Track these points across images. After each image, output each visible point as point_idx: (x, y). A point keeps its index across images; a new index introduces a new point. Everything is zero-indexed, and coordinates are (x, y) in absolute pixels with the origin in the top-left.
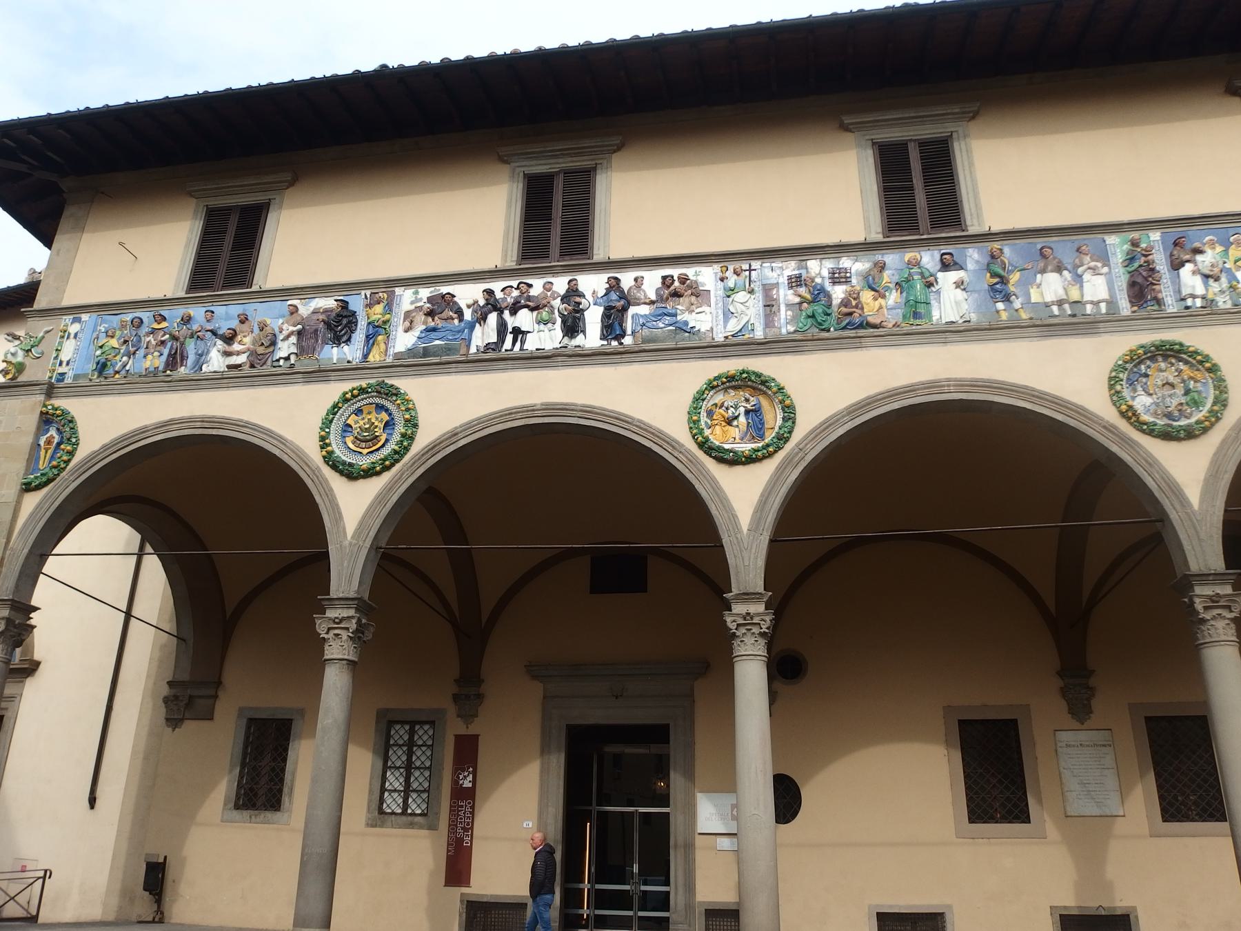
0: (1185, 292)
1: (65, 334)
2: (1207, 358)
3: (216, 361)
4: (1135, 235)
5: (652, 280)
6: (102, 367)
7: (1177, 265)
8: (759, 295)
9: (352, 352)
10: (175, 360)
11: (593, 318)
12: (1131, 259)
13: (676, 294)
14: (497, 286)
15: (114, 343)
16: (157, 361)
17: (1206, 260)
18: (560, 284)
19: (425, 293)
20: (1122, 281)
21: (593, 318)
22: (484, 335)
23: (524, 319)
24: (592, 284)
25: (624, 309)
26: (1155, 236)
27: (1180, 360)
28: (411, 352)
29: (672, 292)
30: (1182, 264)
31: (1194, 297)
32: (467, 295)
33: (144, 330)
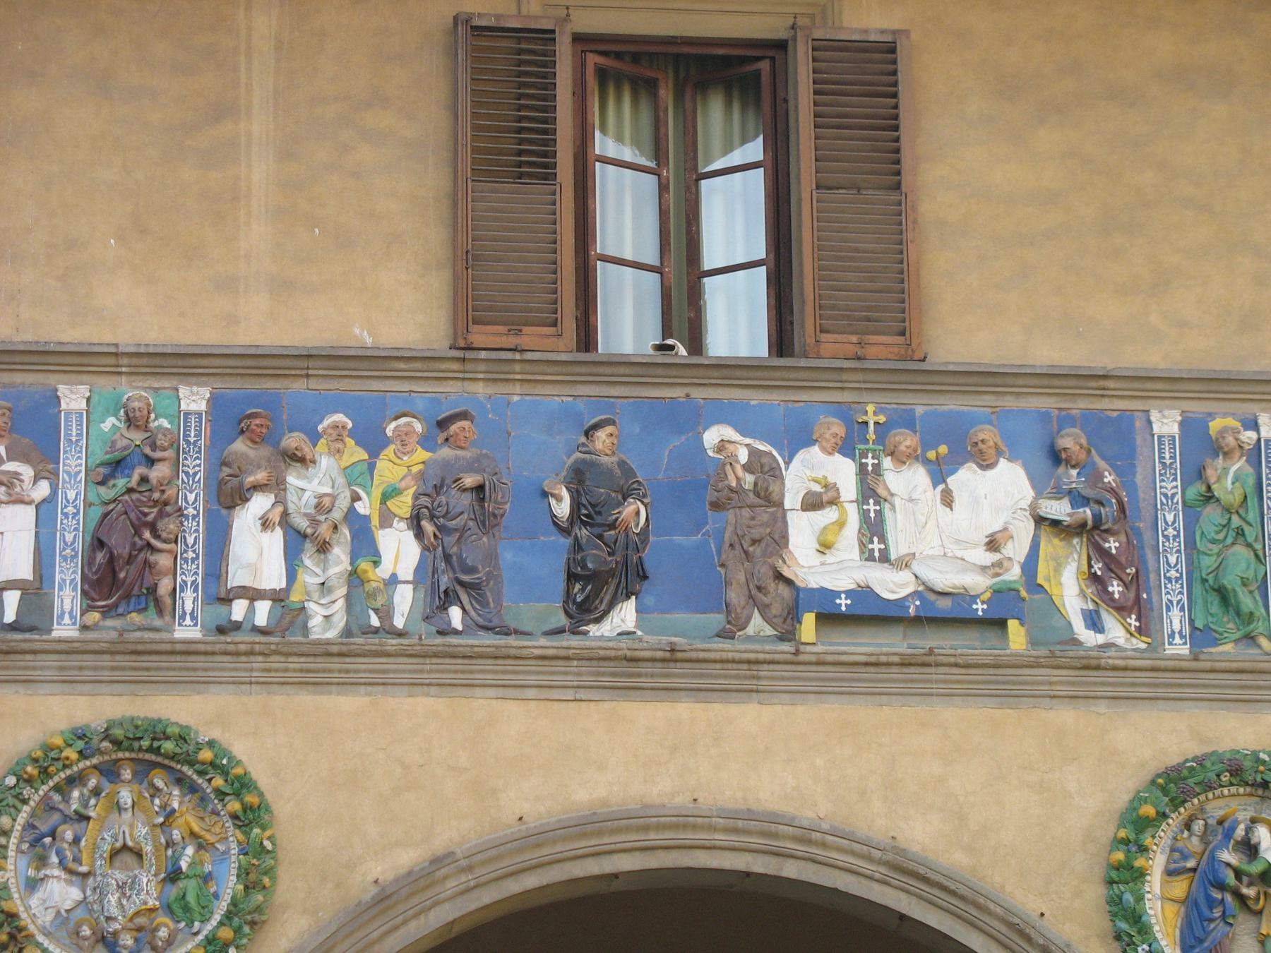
0: (237, 577)
2: (243, 785)
4: (134, 392)
7: (230, 496)
20: (72, 535)
26: (195, 399)
27: (180, 781)
30: (239, 497)
31: (254, 595)
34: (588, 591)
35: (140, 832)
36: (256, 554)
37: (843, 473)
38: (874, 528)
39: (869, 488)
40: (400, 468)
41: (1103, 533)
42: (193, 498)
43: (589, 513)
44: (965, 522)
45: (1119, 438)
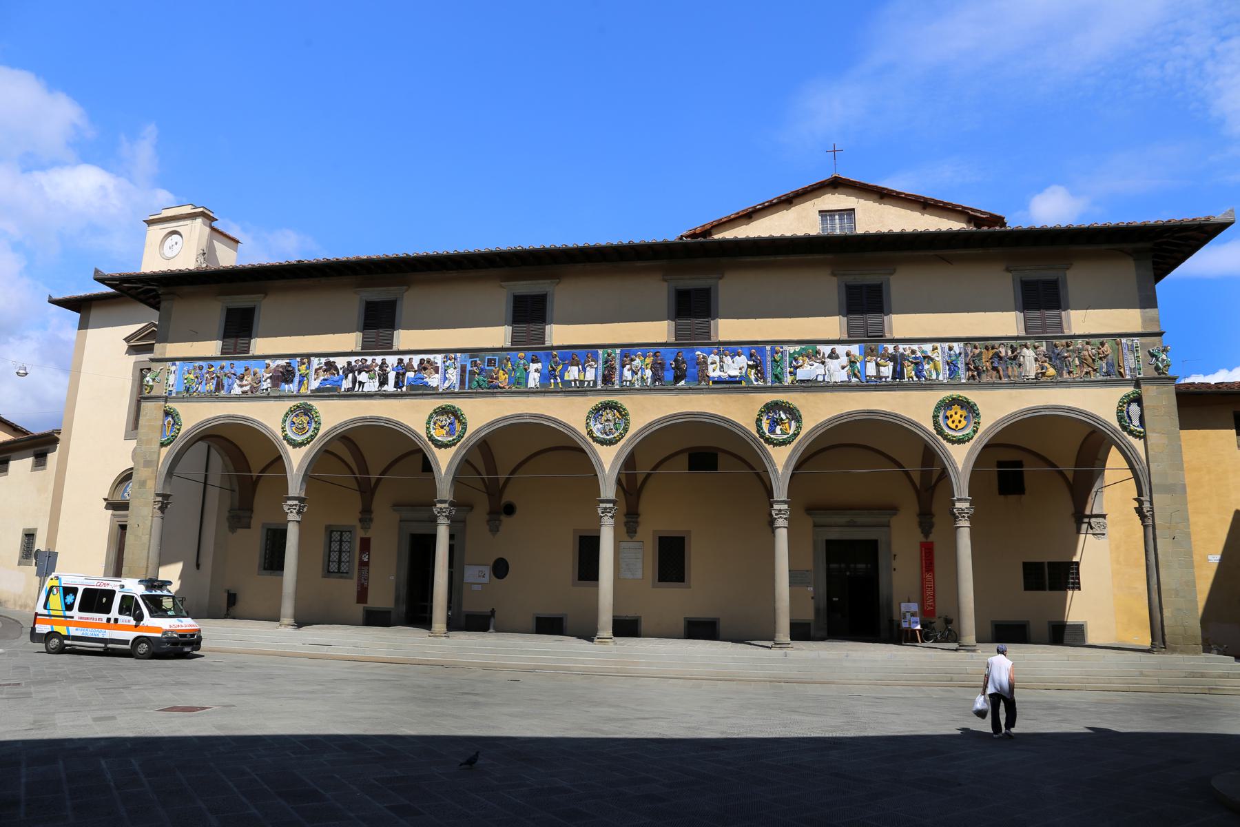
1: (169, 372)
3: (237, 390)
5: (416, 359)
6: (187, 390)
7: (623, 366)
8: (459, 369)
9: (292, 387)
10: (219, 386)
11: (392, 376)
12: (606, 362)
13: (425, 369)
14: (353, 359)
15: (192, 376)
16: (211, 386)
17: (637, 362)
18: (379, 359)
19: (323, 360)
20: (600, 373)
21: (392, 376)
22: (346, 384)
23: (363, 377)
24: (392, 360)
25: (404, 374)
26: (618, 351)
28: (318, 390)
29: (423, 366)
32: (341, 362)
33: (204, 371)
34: (677, 379)
35: (610, 416)
36: (627, 374)
37: (717, 358)
38: (722, 367)
39: (721, 361)
40: (648, 360)
41: (757, 367)
42: (618, 366)
43: (677, 368)
44: (735, 366)
45: (762, 352)
